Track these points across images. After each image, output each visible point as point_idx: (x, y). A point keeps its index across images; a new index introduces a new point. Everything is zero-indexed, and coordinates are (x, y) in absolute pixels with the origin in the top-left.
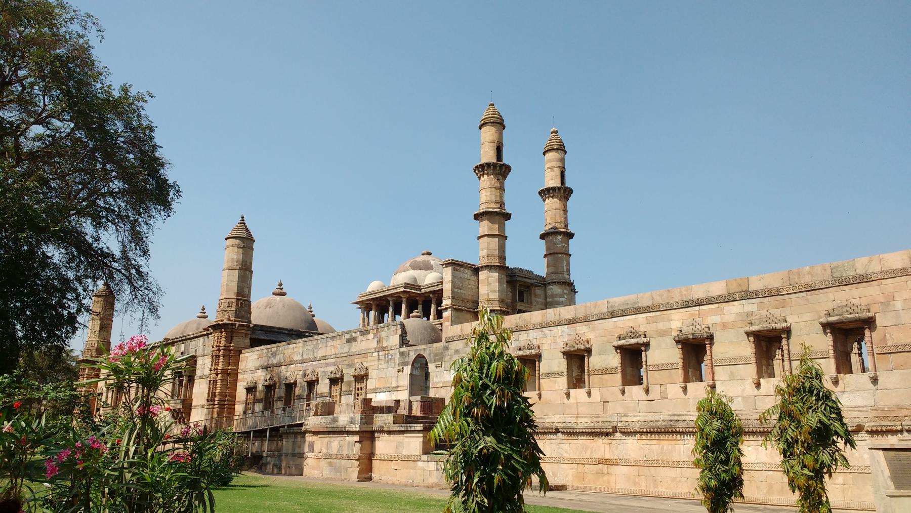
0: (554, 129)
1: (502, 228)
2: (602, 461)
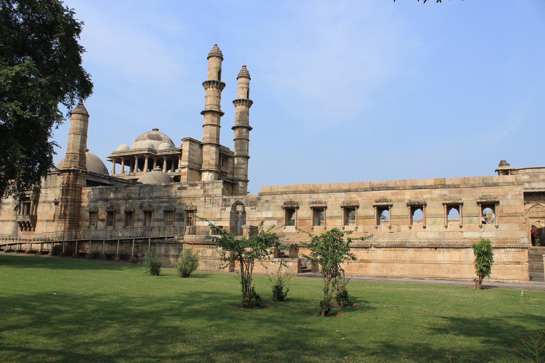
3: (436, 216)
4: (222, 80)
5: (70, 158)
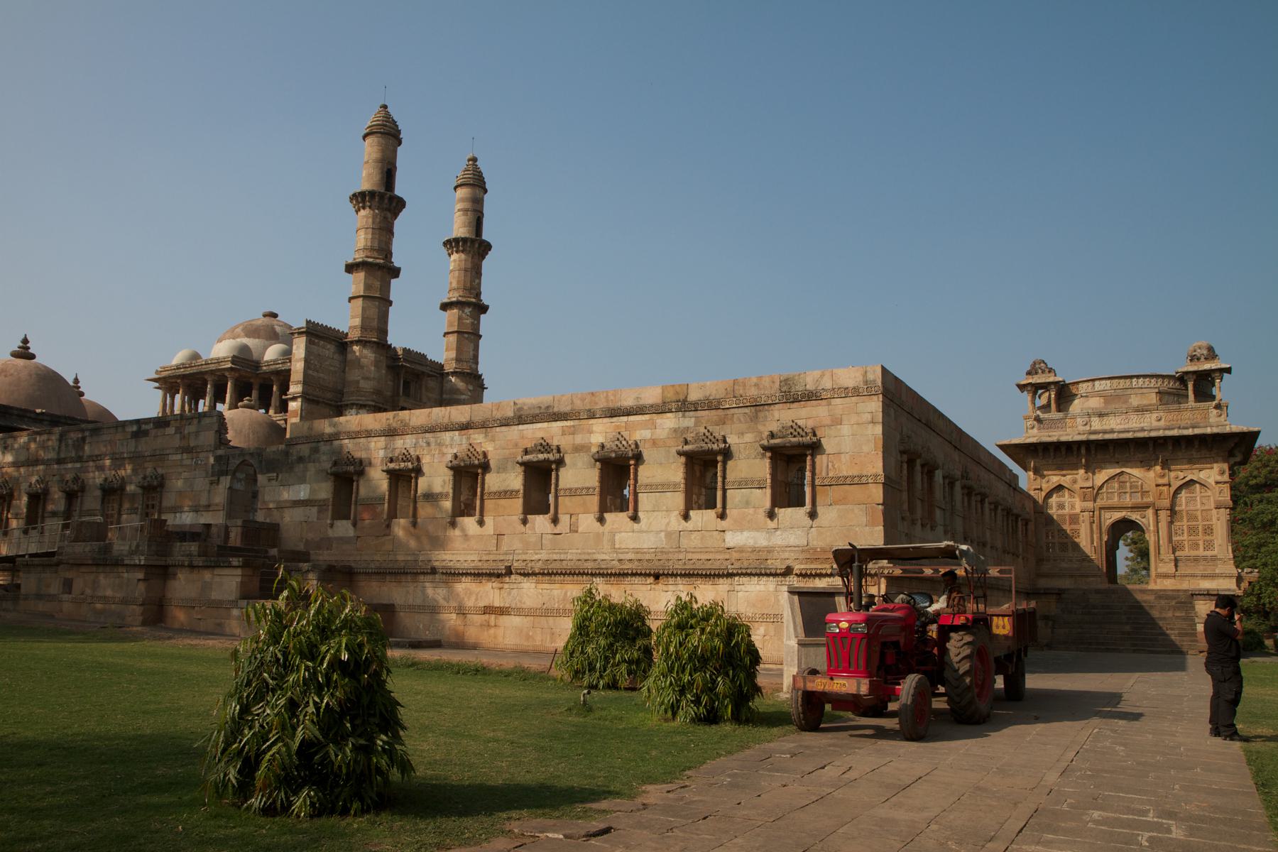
1: (386, 288)
2: (488, 610)
3: (663, 488)
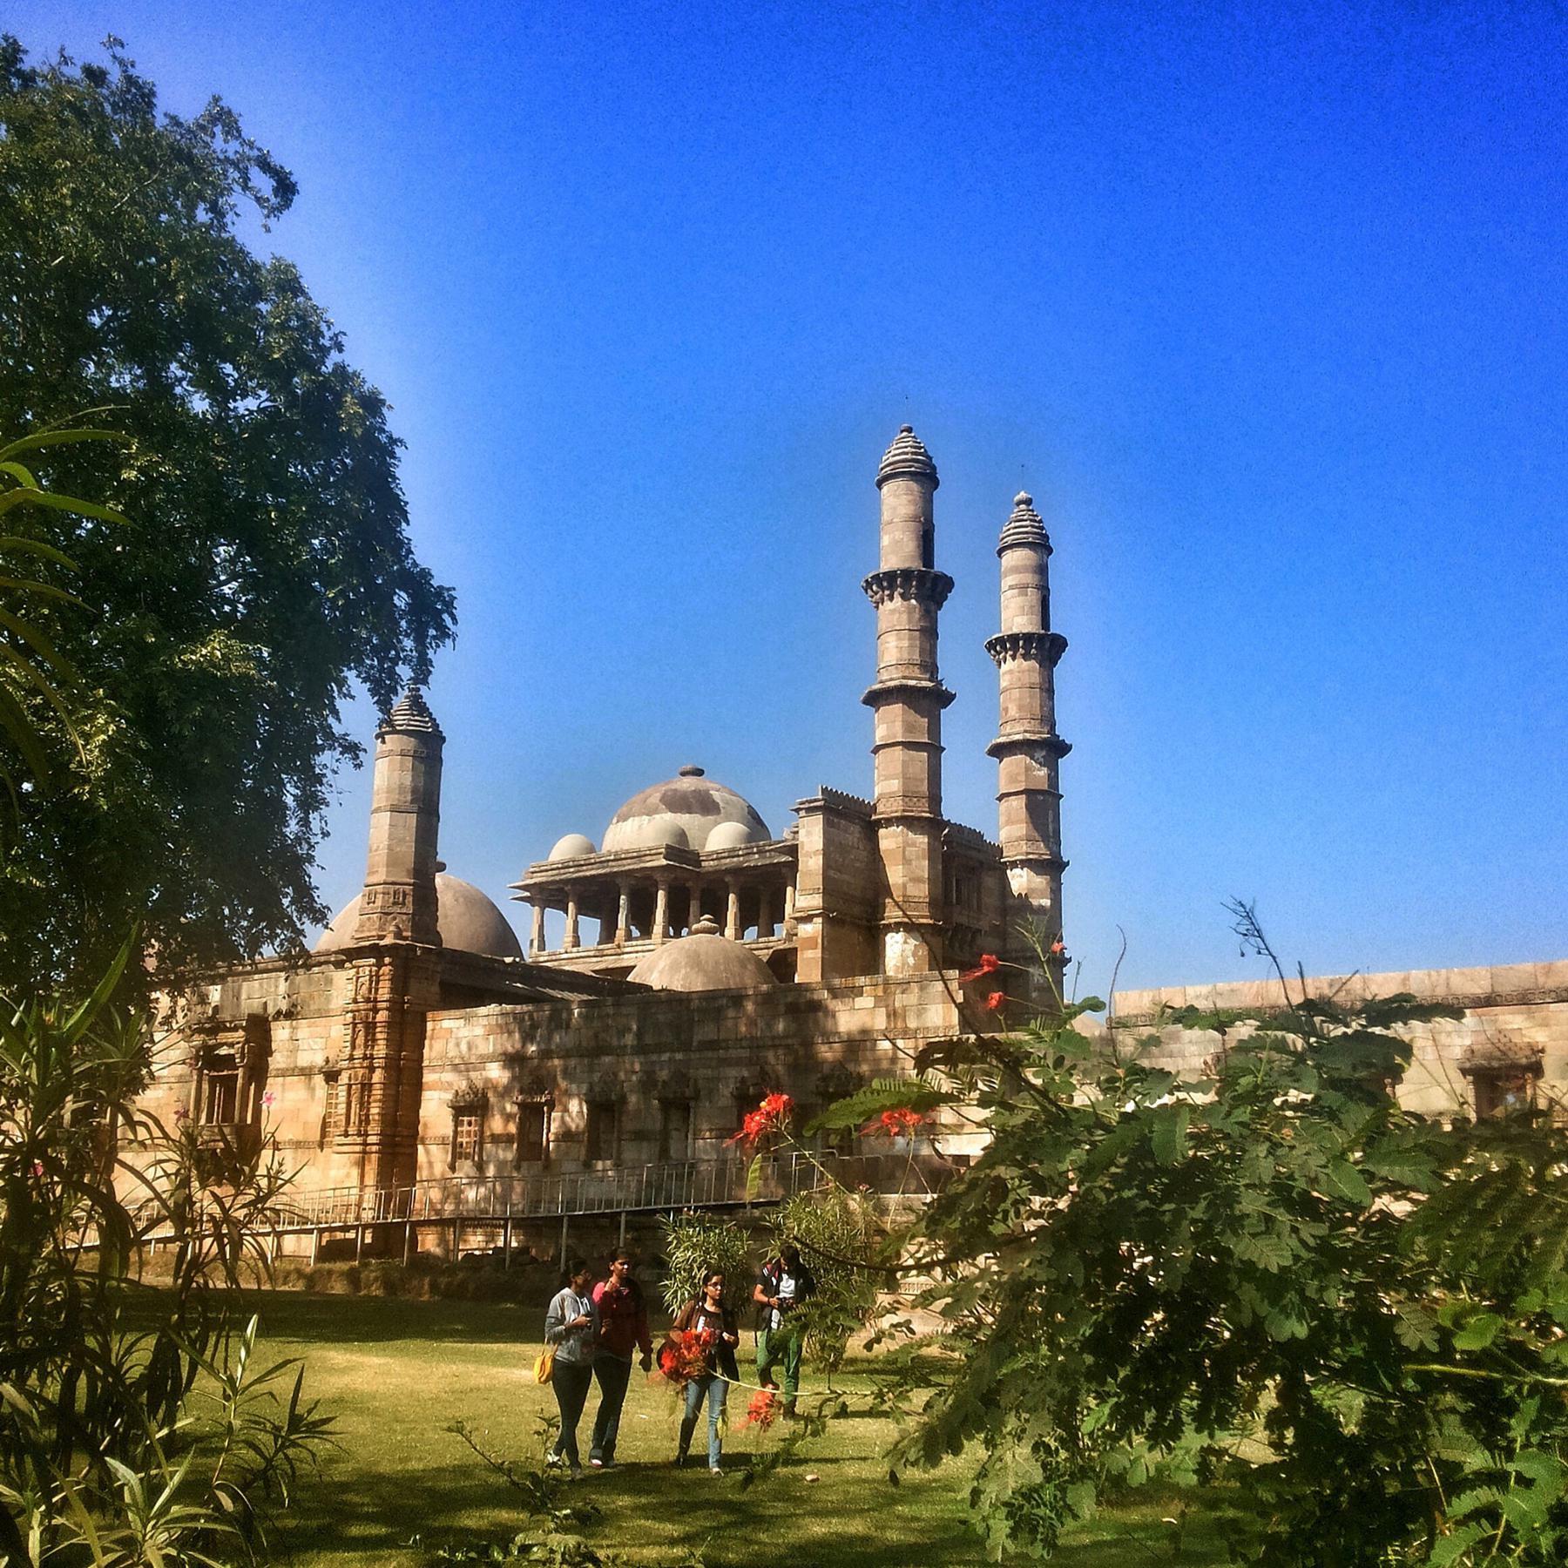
0: (1022, 495)
1: (934, 729)
4: (940, 566)
5: (379, 902)
